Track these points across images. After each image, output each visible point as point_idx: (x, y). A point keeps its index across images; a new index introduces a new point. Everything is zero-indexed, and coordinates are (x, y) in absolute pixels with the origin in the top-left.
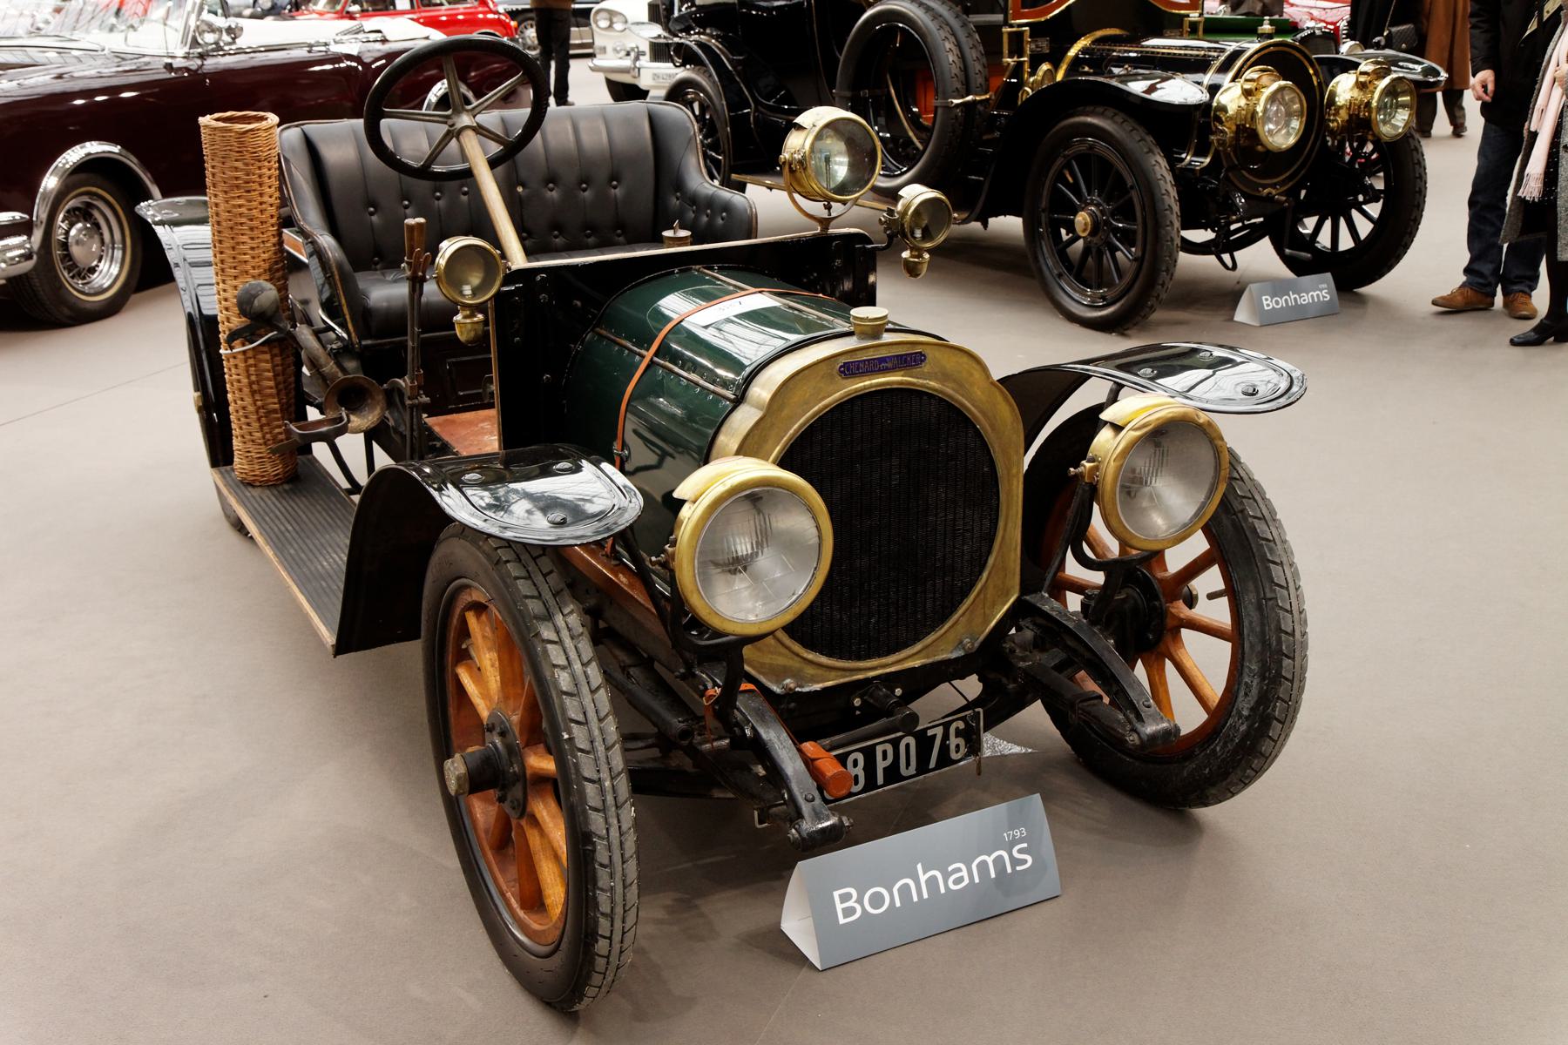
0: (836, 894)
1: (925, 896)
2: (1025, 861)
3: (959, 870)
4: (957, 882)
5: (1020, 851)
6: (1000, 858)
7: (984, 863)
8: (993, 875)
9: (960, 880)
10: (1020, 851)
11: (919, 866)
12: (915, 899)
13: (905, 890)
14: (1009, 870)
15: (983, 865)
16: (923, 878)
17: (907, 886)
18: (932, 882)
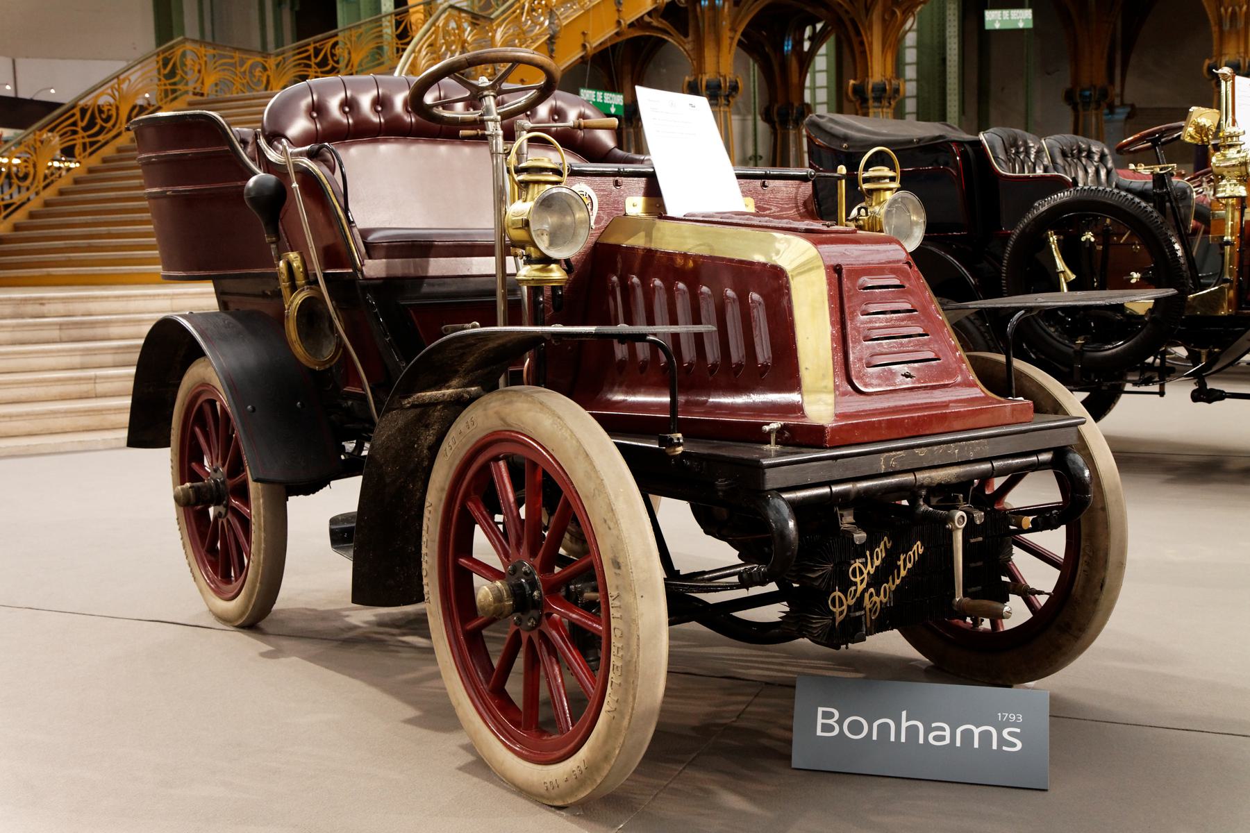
0: (820, 710)
1: (903, 740)
3: (944, 730)
4: (937, 738)
5: (1010, 734)
6: (989, 733)
7: (971, 732)
8: (976, 745)
9: (942, 738)
10: (1010, 734)
11: (904, 713)
12: (892, 739)
14: (995, 747)
15: (968, 735)
16: (904, 724)
17: (888, 725)
18: (912, 731)
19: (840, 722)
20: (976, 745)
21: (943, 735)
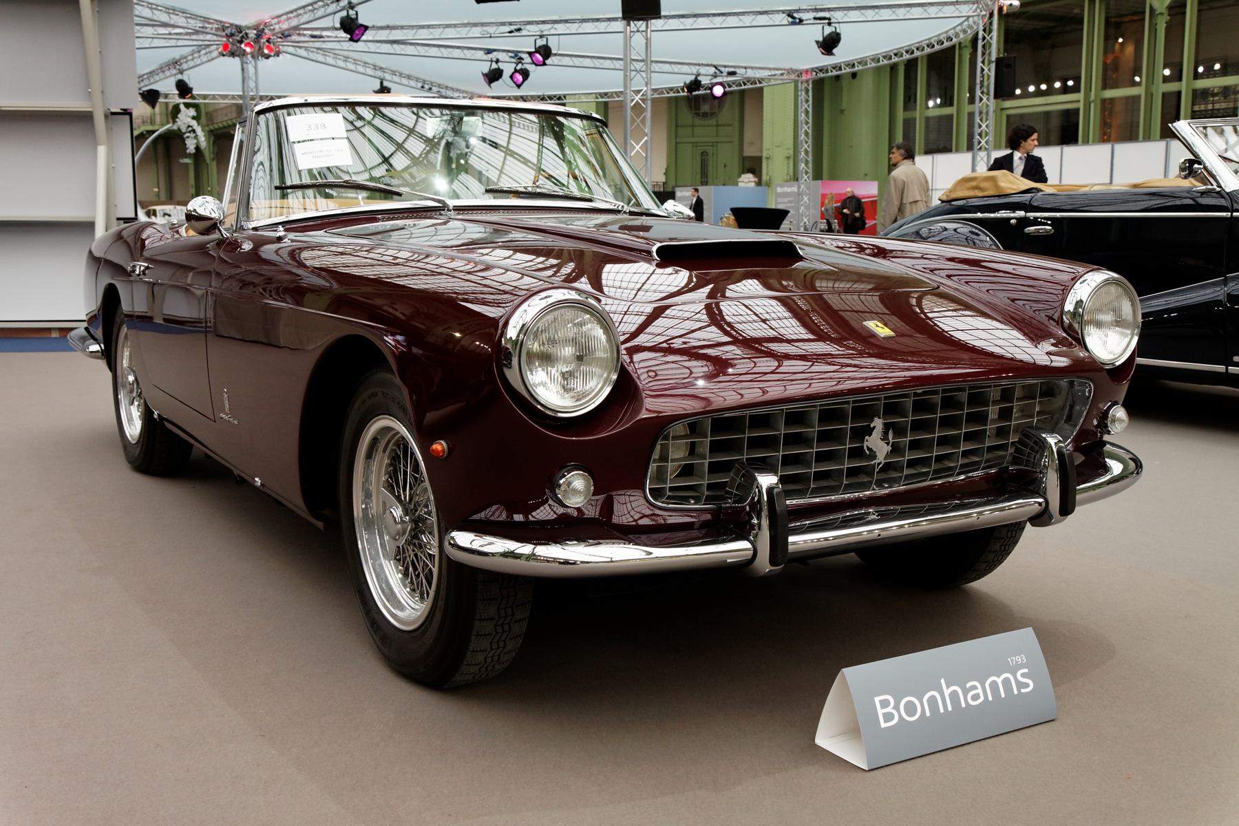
1: (950, 709)
4: (975, 697)
5: (1023, 675)
10: (1023, 675)
12: (942, 711)
13: (932, 700)
15: (994, 684)
16: (947, 692)
17: (933, 697)
18: (954, 695)
19: (897, 707)
21: (977, 694)
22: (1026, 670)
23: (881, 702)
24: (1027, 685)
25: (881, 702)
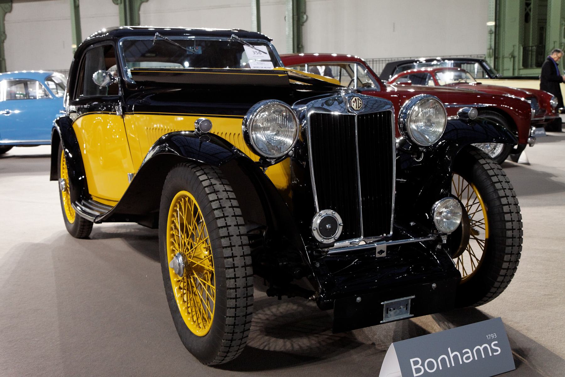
1: (453, 365)
2: (497, 351)
3: (467, 353)
4: (468, 358)
5: (495, 345)
7: (478, 350)
8: (483, 357)
10: (494, 345)
12: (449, 366)
13: (443, 360)
14: (491, 355)
15: (478, 351)
16: (451, 356)
17: (444, 359)
18: (455, 357)
19: (423, 365)
20: (483, 357)
21: (469, 356)
22: (497, 342)
23: (413, 361)
24: (497, 351)
25: (413, 361)
